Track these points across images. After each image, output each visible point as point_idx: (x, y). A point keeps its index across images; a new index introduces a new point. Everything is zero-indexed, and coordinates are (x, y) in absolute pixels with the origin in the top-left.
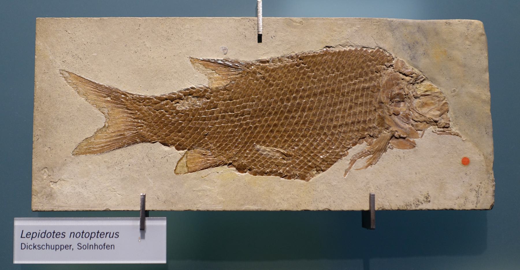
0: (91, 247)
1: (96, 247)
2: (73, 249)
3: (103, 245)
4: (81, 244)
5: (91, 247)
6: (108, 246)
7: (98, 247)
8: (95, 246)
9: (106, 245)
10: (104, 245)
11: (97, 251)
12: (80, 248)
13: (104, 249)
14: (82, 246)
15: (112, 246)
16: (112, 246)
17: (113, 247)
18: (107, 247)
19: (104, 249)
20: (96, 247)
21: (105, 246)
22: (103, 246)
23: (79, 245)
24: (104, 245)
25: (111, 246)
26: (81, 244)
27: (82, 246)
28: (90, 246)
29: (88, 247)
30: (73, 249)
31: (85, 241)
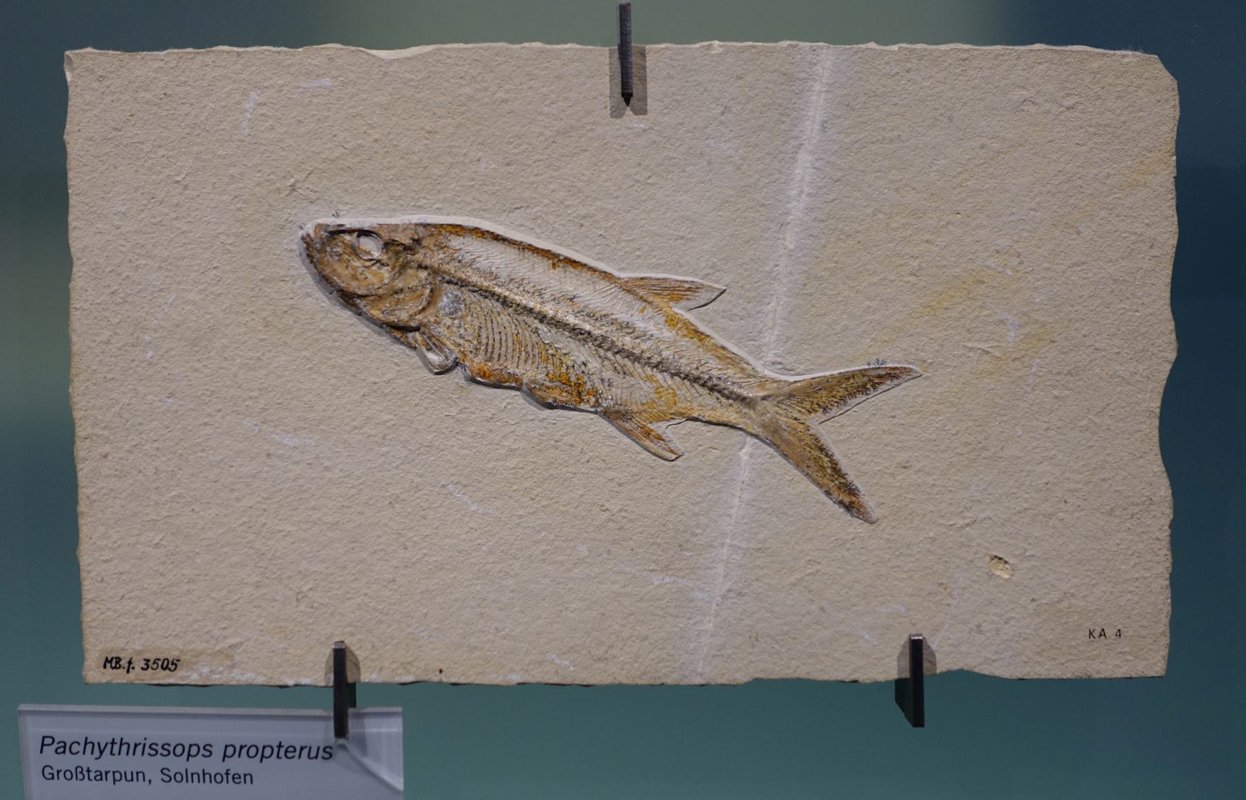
0: (195, 777)
1: (207, 777)
2: (150, 781)
3: (223, 772)
4: (169, 770)
5: (195, 777)
6: (236, 776)
7: (213, 778)
8: (204, 774)
9: (232, 773)
10: (227, 774)
11: (208, 787)
12: (167, 779)
13: (228, 782)
14: (172, 774)
15: (248, 777)
16: (248, 777)
17: (248, 778)
18: (233, 778)
19: (228, 782)
20: (207, 777)
21: (230, 777)
22: (225, 777)
23: (165, 771)
24: (227, 774)
25: (245, 775)
26: (169, 770)
27: (172, 774)
28: (192, 774)
29: (187, 777)
30: (150, 781)
31: (176, 764)
